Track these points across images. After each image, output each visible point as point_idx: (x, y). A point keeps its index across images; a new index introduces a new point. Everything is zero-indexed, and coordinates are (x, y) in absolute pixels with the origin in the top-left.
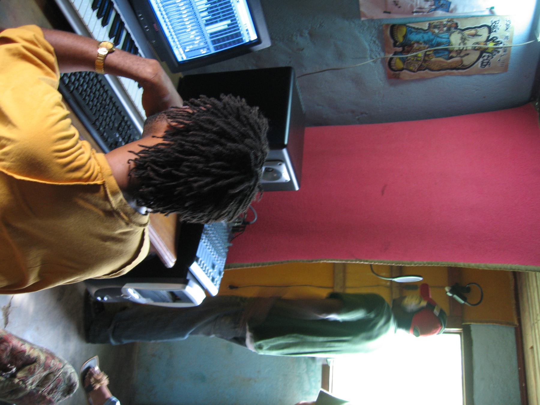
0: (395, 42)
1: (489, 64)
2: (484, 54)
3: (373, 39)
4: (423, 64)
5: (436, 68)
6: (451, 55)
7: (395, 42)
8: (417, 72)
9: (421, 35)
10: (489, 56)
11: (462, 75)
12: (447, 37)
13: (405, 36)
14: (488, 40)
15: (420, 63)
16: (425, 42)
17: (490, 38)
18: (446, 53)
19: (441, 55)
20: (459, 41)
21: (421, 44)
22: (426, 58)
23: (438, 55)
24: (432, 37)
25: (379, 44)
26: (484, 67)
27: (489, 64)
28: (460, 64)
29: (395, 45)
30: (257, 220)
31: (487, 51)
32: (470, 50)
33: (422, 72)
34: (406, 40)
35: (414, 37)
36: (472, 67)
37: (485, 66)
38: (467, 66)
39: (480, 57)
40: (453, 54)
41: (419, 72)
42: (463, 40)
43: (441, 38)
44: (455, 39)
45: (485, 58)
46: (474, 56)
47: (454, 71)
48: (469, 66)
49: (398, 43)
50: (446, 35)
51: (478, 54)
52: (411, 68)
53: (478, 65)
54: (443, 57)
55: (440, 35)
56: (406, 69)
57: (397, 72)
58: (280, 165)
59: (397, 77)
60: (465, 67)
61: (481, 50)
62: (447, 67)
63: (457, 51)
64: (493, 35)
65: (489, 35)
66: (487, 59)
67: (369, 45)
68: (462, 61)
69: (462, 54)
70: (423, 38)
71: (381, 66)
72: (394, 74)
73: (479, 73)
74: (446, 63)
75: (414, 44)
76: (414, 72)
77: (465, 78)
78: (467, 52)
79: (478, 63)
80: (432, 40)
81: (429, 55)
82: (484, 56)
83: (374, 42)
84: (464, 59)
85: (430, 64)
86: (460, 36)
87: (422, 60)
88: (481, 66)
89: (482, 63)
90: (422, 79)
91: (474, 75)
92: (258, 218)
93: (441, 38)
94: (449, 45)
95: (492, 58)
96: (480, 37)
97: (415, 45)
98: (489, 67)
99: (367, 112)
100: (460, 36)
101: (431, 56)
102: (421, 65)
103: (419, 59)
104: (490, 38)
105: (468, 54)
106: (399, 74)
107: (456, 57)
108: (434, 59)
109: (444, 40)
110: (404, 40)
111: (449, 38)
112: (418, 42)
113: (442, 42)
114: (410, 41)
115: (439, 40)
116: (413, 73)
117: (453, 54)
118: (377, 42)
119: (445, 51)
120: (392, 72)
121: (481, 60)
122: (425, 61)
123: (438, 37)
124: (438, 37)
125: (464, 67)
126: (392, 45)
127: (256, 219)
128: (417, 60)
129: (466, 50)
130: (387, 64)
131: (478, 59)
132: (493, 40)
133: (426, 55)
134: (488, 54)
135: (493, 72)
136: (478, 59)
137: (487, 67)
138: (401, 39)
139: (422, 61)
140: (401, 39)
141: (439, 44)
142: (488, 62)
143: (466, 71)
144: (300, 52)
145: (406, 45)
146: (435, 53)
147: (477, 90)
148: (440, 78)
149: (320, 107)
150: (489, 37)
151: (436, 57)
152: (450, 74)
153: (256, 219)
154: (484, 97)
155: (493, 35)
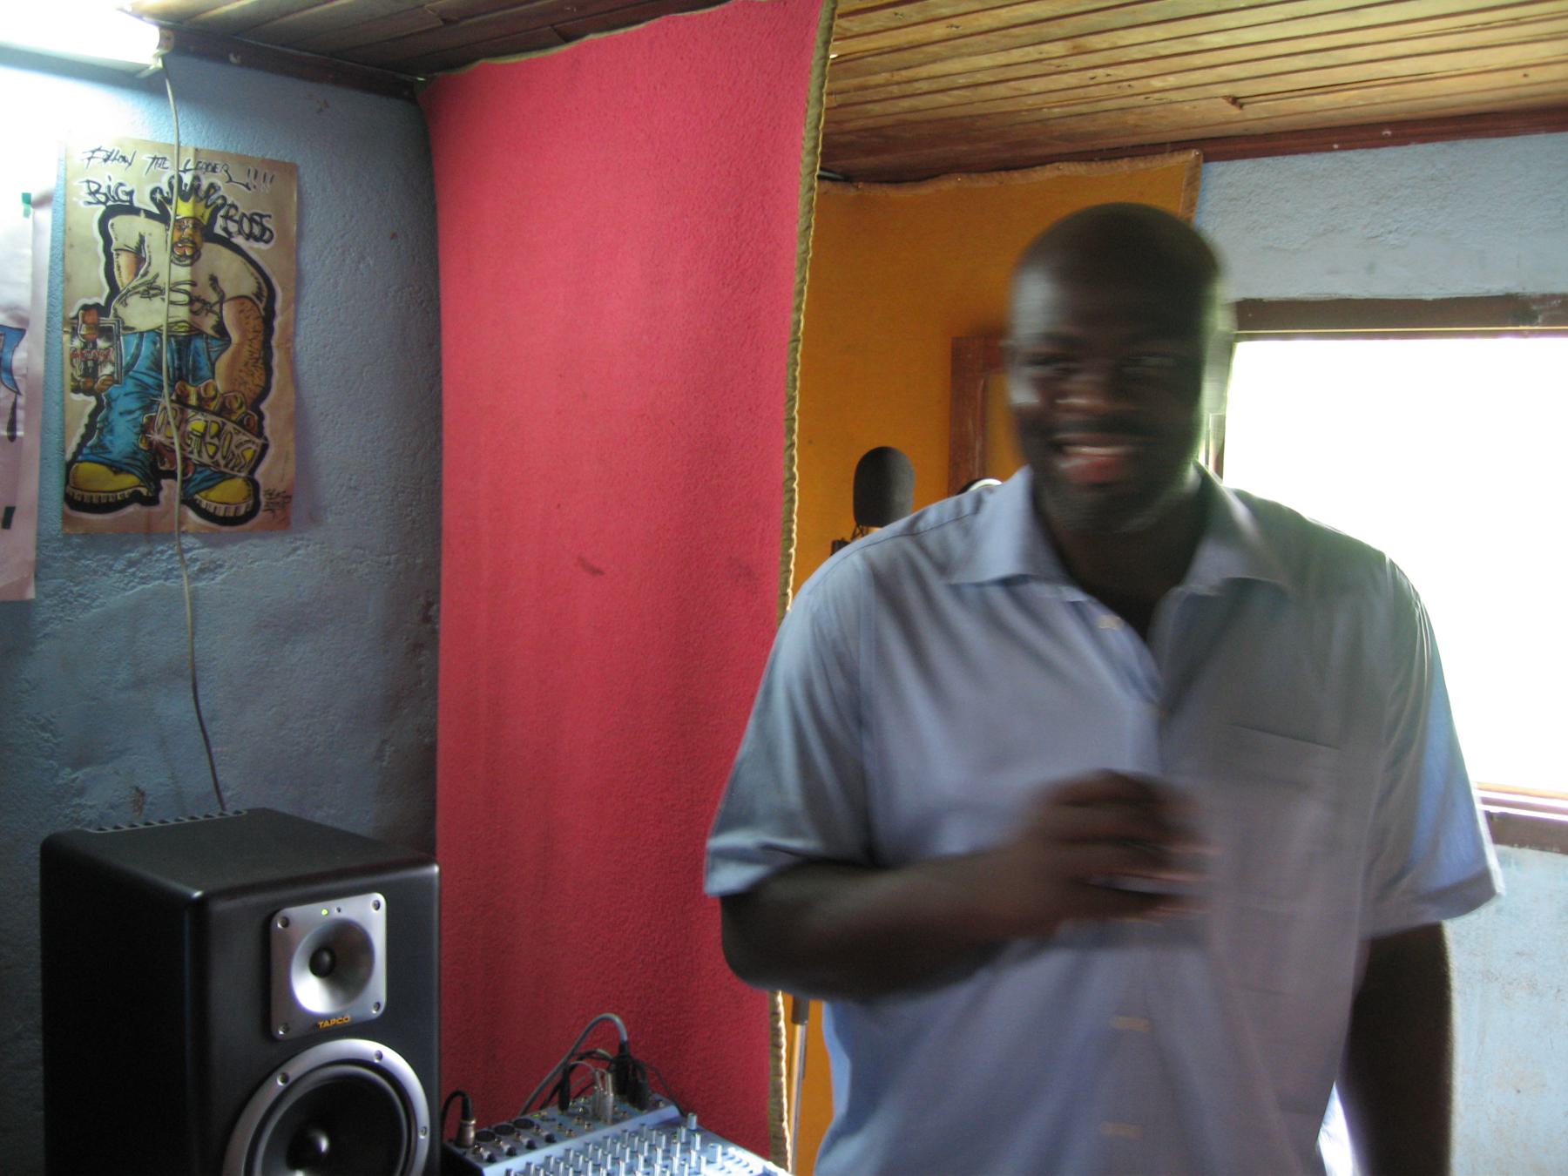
0: (136, 498)
1: (261, 216)
2: (218, 230)
3: (119, 566)
4: (234, 418)
5: (259, 379)
6: (210, 332)
7: (136, 498)
8: (266, 439)
9: (114, 416)
10: (227, 217)
11: (296, 300)
12: (134, 341)
13: (116, 468)
14: (163, 217)
15: (230, 427)
16: (147, 408)
17: (155, 210)
18: (199, 344)
19: (203, 360)
20: (157, 301)
21: (152, 419)
22: (214, 405)
23: (206, 372)
24: (130, 385)
25: (144, 549)
26: (271, 232)
27: (257, 218)
28: (249, 304)
29: (152, 501)
30: (622, 1018)
31: (205, 221)
32: (193, 273)
33: (267, 422)
34: (127, 464)
35: (123, 438)
36: (267, 271)
37: (264, 229)
38: (259, 283)
39: (226, 242)
40: (208, 323)
41: (267, 432)
42: (151, 290)
43: (136, 357)
44: (144, 315)
45: (233, 227)
46: (220, 260)
47: (277, 323)
48: (261, 281)
49: (144, 491)
50: (128, 346)
51: (210, 250)
52: (248, 454)
53: (258, 251)
54: (213, 359)
55: (126, 359)
56: (252, 471)
57: (263, 499)
58: (286, 923)
59: (282, 502)
60: (265, 294)
61: (198, 239)
62: (257, 345)
63: (193, 313)
64: (143, 201)
65: (143, 214)
66: (240, 223)
67: (144, 580)
68: (240, 298)
69: (213, 297)
70: (130, 412)
71: (234, 549)
72: (269, 509)
73: (293, 250)
74: (240, 345)
75: (150, 444)
76: (265, 447)
77: (310, 295)
78: (204, 280)
79: (251, 248)
80: (144, 387)
81: (199, 398)
82: (226, 229)
83: (132, 564)
84: (230, 292)
85: (239, 395)
86: (134, 300)
87: (219, 420)
88: (267, 242)
89: (249, 236)
90: (299, 420)
91: (297, 262)
92: (616, 1013)
93: (136, 357)
94: (160, 335)
95: (236, 208)
96: (147, 239)
97: (157, 437)
98: (270, 216)
99: (422, 600)
100: (134, 300)
101: (205, 391)
102: (240, 423)
103: (214, 429)
104: (155, 210)
105: (214, 280)
106: (269, 493)
107: (221, 318)
108: (220, 384)
109: (146, 349)
110: (129, 472)
111: (142, 334)
112: (145, 430)
113: (152, 353)
114: (135, 453)
115: (142, 364)
116: (271, 451)
117: (208, 323)
118: (134, 555)
119: (192, 347)
120: (261, 515)
121: (239, 240)
122: (224, 411)
123: (130, 366)
124: (130, 366)
125: (266, 291)
126: (145, 510)
127: (617, 1020)
128: (218, 435)
129: (193, 284)
130: (226, 529)
131: (237, 249)
132: (163, 203)
133: (201, 408)
134: (220, 222)
135: (294, 208)
136: (237, 249)
137: (267, 223)
138: (128, 481)
139: (224, 420)
140: (128, 481)
141: (157, 365)
142: (251, 220)
143: (283, 289)
144: (149, 799)
145: (153, 466)
146: (194, 381)
147: (362, 258)
148: (303, 366)
149: (389, 750)
150: (149, 215)
151: (213, 377)
152: (289, 339)
153: (617, 1020)
154: (394, 236)
155: (143, 201)
